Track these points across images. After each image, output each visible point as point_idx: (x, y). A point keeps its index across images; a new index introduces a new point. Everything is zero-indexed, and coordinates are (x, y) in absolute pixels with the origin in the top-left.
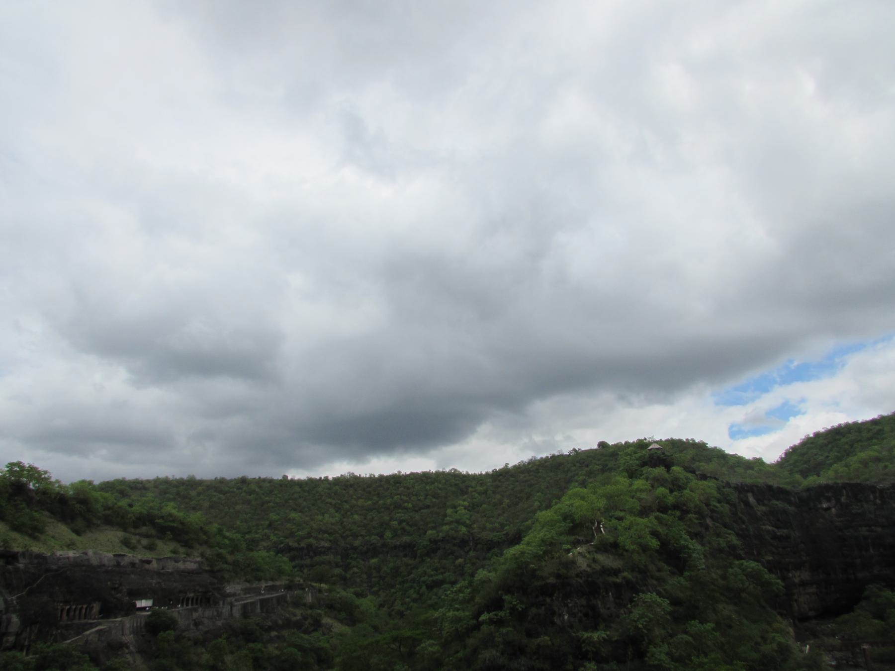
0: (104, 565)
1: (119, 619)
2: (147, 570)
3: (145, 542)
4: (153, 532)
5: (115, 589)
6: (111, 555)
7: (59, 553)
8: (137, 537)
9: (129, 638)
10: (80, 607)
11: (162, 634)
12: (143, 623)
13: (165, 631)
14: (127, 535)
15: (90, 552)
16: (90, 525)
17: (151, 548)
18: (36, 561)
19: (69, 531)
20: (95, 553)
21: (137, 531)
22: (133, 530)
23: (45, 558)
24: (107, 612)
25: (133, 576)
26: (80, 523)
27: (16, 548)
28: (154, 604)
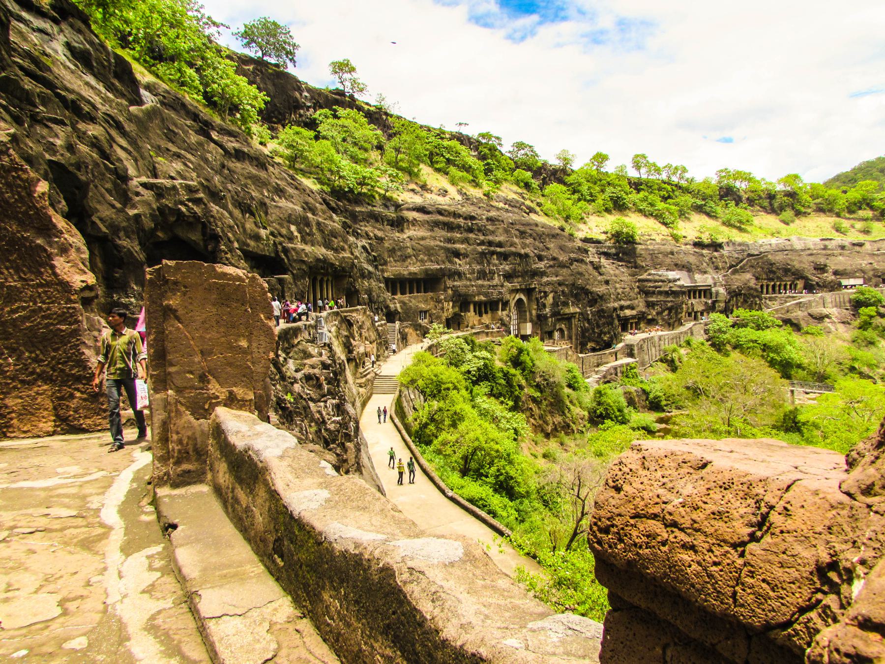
0: (809, 249)
1: (820, 295)
2: (858, 252)
3: (859, 225)
4: (869, 213)
5: (821, 269)
6: (817, 240)
7: (760, 242)
8: (852, 222)
9: (833, 311)
10: (783, 283)
11: (863, 310)
12: (847, 299)
13: (867, 307)
14: (838, 219)
15: (793, 238)
16: (798, 213)
17: (866, 232)
18: (739, 248)
19: (778, 221)
20: (799, 239)
21: (851, 216)
22: (847, 215)
23: (747, 245)
24: (810, 288)
25: (841, 258)
26: (788, 214)
27: (721, 239)
28: (865, 283)
